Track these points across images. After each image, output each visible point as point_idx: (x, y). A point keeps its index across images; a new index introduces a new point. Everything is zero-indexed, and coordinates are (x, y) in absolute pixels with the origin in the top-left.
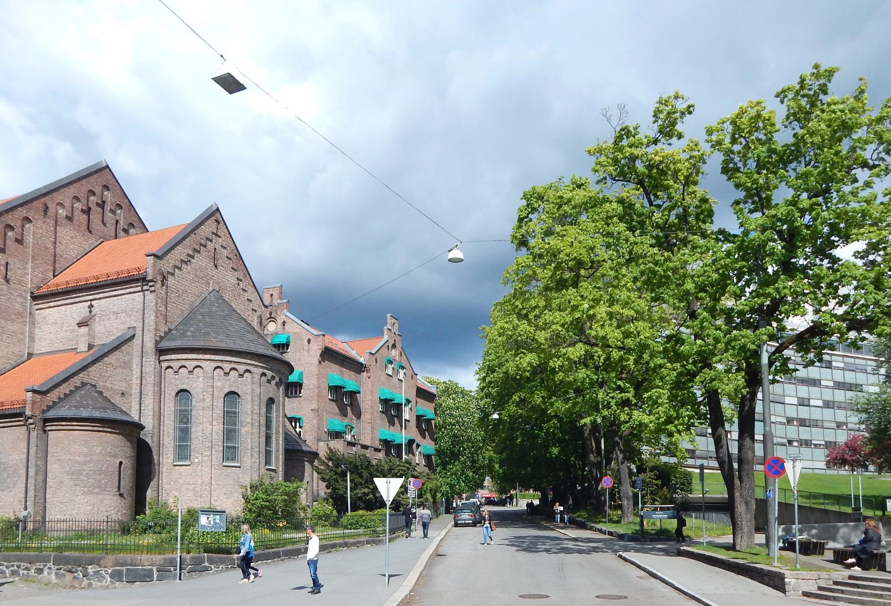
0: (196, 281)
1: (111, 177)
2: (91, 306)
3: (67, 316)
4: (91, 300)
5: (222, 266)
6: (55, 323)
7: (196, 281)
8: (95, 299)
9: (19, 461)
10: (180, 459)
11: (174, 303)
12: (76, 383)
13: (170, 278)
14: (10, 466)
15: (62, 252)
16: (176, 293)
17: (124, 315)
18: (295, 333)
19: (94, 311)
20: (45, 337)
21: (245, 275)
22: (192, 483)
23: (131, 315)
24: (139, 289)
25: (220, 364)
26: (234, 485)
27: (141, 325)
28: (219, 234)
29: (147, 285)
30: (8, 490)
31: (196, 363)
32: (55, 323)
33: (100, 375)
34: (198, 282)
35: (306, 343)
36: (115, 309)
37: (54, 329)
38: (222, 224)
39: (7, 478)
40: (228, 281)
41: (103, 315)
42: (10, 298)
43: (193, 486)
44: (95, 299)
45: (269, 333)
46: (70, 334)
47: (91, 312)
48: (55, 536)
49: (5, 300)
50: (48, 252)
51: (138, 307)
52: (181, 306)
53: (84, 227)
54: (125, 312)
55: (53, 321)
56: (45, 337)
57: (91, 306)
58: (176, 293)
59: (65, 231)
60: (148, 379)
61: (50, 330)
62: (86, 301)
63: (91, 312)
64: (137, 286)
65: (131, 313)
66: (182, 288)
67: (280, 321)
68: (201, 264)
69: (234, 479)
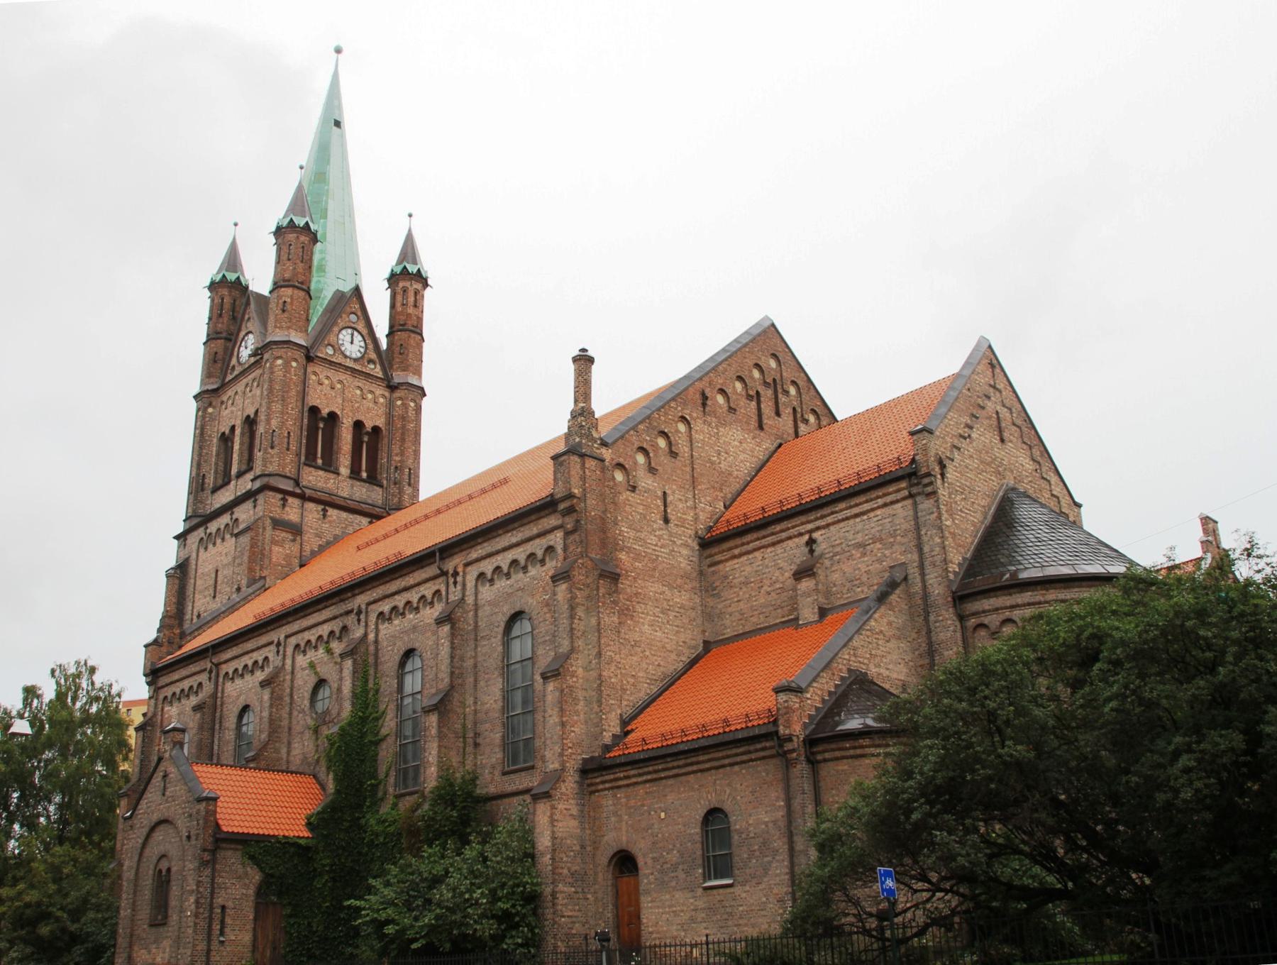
2: (811, 542)
3: (767, 567)
4: (810, 532)
6: (746, 583)
9: (771, 825)
11: (961, 511)
14: (752, 835)
15: (731, 467)
17: (878, 545)
19: (818, 549)
20: (730, 610)
23: (892, 544)
24: (906, 493)
27: (916, 557)
29: (918, 484)
30: (755, 881)
32: (746, 583)
36: (859, 538)
37: (744, 593)
39: (749, 859)
41: (835, 555)
44: (818, 528)
46: (776, 597)
47: (812, 551)
51: (904, 527)
53: (754, 423)
54: (880, 540)
55: (742, 579)
56: (730, 610)
57: (811, 542)
60: (946, 653)
61: (738, 595)
62: (801, 534)
63: (812, 551)
64: (898, 491)
65: (892, 540)
66: (968, 484)
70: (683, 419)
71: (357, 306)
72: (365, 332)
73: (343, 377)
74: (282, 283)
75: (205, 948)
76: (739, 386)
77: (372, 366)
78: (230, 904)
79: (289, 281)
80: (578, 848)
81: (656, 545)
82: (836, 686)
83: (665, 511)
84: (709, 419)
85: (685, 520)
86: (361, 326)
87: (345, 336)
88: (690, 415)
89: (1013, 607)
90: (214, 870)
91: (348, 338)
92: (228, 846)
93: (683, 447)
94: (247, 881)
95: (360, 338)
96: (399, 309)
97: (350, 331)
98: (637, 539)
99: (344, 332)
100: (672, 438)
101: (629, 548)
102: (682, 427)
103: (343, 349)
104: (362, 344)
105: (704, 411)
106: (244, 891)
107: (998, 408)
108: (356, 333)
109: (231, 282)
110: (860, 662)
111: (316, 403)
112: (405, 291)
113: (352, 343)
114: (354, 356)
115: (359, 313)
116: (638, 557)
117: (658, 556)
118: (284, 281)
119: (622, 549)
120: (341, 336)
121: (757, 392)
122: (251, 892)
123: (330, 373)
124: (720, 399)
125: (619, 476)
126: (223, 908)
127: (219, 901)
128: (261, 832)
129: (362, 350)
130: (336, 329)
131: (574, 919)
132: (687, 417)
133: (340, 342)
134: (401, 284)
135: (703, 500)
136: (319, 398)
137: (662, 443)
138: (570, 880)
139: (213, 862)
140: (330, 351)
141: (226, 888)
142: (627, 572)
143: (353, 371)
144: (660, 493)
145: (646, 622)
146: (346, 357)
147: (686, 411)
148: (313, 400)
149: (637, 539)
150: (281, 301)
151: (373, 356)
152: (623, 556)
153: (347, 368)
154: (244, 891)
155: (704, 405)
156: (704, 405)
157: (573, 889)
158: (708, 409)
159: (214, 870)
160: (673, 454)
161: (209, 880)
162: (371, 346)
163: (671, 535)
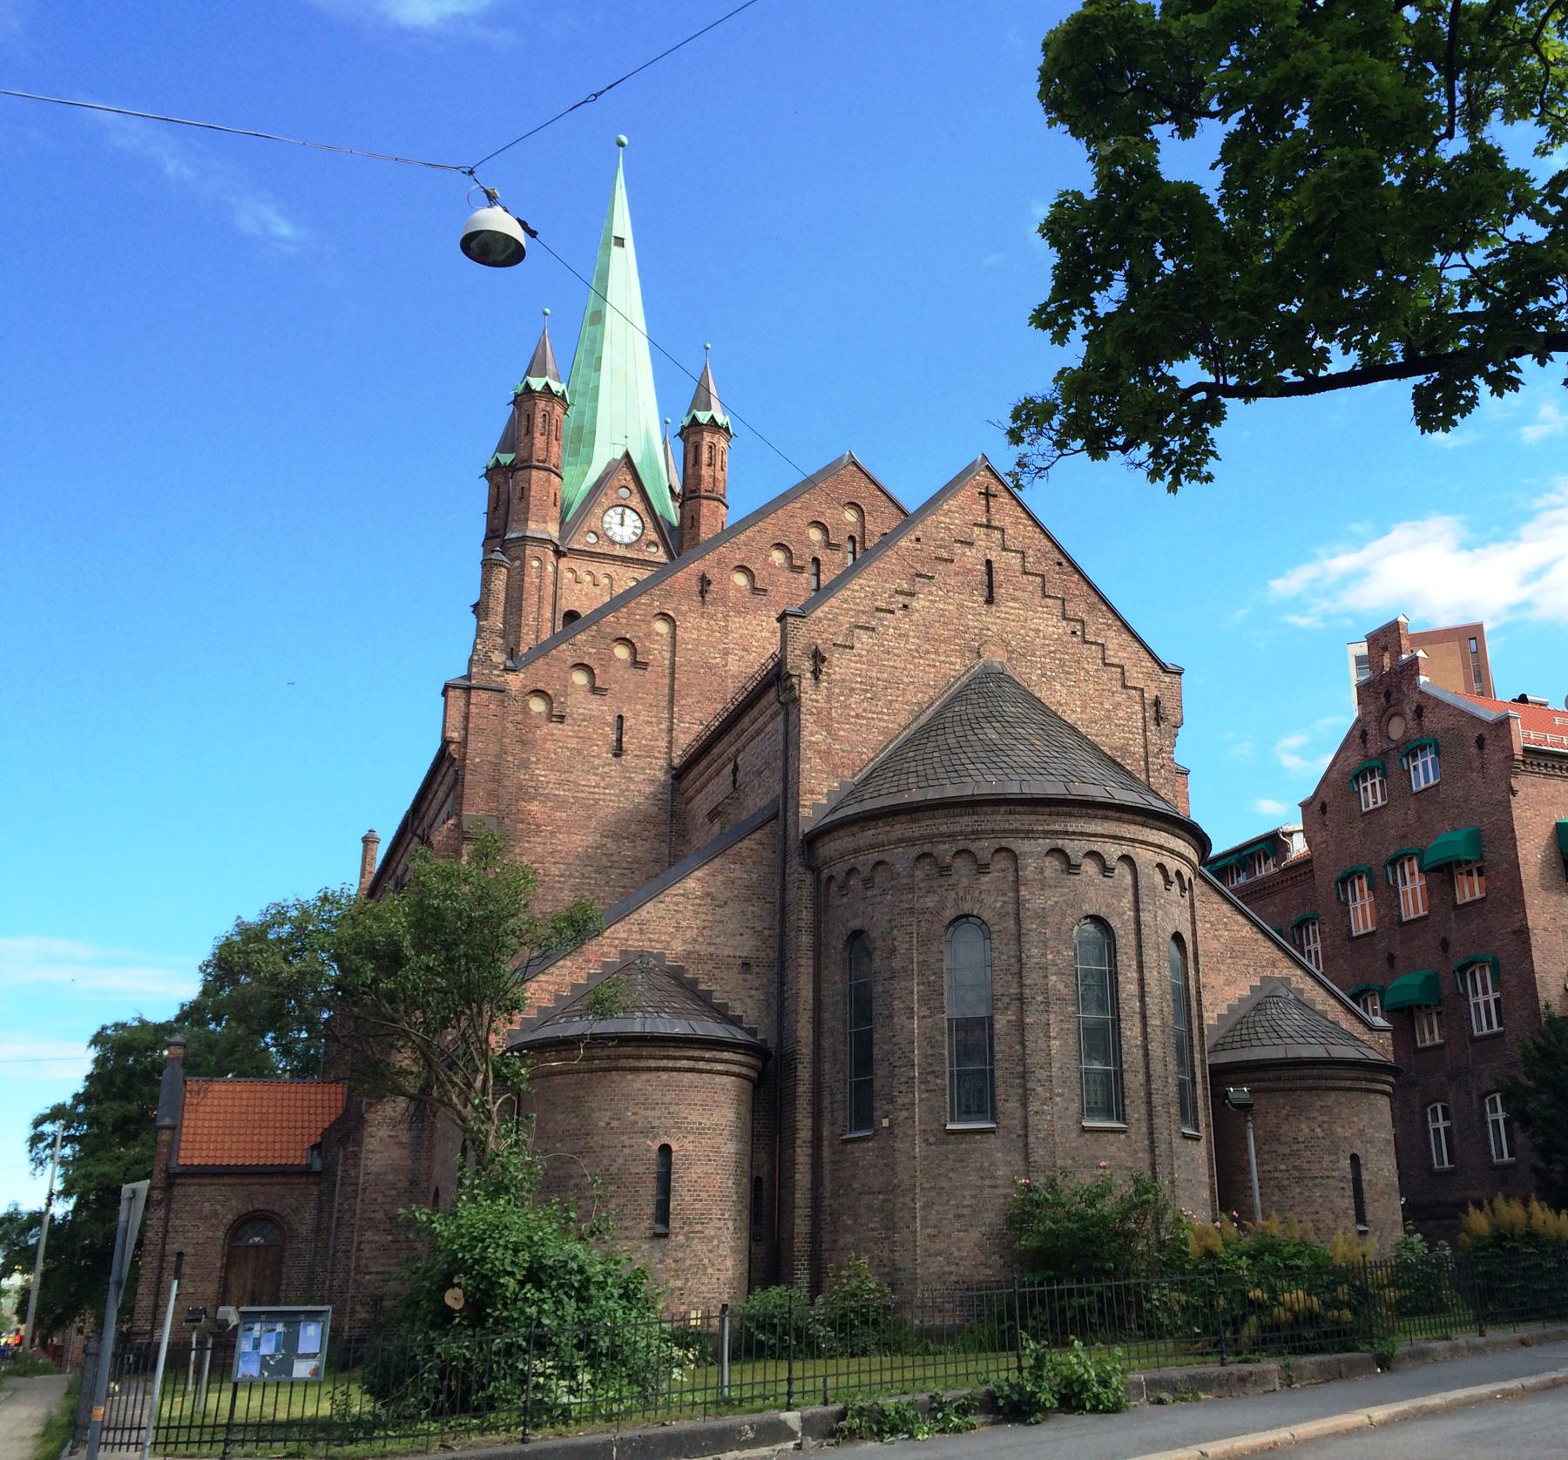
0: (928, 652)
1: (864, 482)
2: (736, 770)
5: (1015, 599)
7: (928, 652)
8: (738, 752)
10: (965, 1113)
11: (857, 716)
12: (604, 955)
13: (835, 657)
16: (866, 691)
18: (1447, 730)
21: (1091, 608)
22: (876, 1188)
25: (927, 848)
26: (981, 1188)
28: (993, 523)
31: (875, 856)
33: (677, 928)
34: (937, 653)
35: (1474, 750)
38: (1004, 498)
40: (1038, 630)
42: (627, 790)
43: (881, 1197)
44: (738, 752)
45: (1393, 746)
48: (284, 1398)
49: (615, 795)
50: (714, 675)
52: (880, 720)
58: (866, 691)
59: (755, 622)
67: (1409, 710)
68: (941, 606)
69: (981, 1168)
70: (664, 616)
71: (629, 477)
72: (640, 507)
73: (610, 568)
74: (520, 465)
75: (152, 1303)
76: (778, 557)
77: (653, 549)
78: (190, 1250)
79: (526, 461)
80: (406, 1184)
81: (597, 786)
82: (590, 976)
83: (619, 740)
84: (711, 609)
85: (653, 748)
86: (635, 501)
87: (613, 517)
88: (674, 610)
89: (857, 851)
90: (168, 1210)
91: (617, 519)
92: (190, 1181)
93: (658, 653)
94: (216, 1222)
95: (635, 516)
96: (690, 471)
97: (619, 510)
98: (560, 783)
99: (611, 512)
100: (638, 645)
101: (546, 796)
102: (661, 627)
103: (610, 534)
104: (639, 524)
105: (703, 602)
106: (211, 1234)
107: (992, 556)
108: (628, 511)
109: (505, 466)
110: (651, 940)
111: (574, 606)
112: (697, 448)
113: (622, 525)
114: (627, 540)
115: (632, 486)
116: (561, 804)
117: (597, 801)
118: (522, 461)
119: (534, 798)
120: (607, 518)
121: (816, 561)
122: (220, 1234)
123: (594, 566)
124: (740, 580)
125: (537, 706)
126: (180, 1255)
127: (174, 1247)
128: (233, 1162)
129: (639, 532)
130: (599, 511)
131: (387, 1276)
132: (671, 613)
133: (606, 526)
134: (691, 439)
135: (687, 718)
136: (578, 599)
137: (622, 652)
138: (387, 1226)
139: (168, 1201)
140: (592, 539)
141: (185, 1232)
142: (538, 826)
143: (624, 560)
144: (610, 719)
145: (567, 886)
146: (614, 543)
147: (667, 606)
148: (566, 604)
149: (560, 783)
150: (518, 488)
151: (654, 536)
152: (534, 807)
153: (614, 558)
154: (211, 1234)
155: (703, 593)
156: (703, 593)
157: (390, 1238)
158: (708, 597)
159: (168, 1210)
160: (637, 663)
161: (161, 1223)
162: (649, 525)
163: (625, 769)
